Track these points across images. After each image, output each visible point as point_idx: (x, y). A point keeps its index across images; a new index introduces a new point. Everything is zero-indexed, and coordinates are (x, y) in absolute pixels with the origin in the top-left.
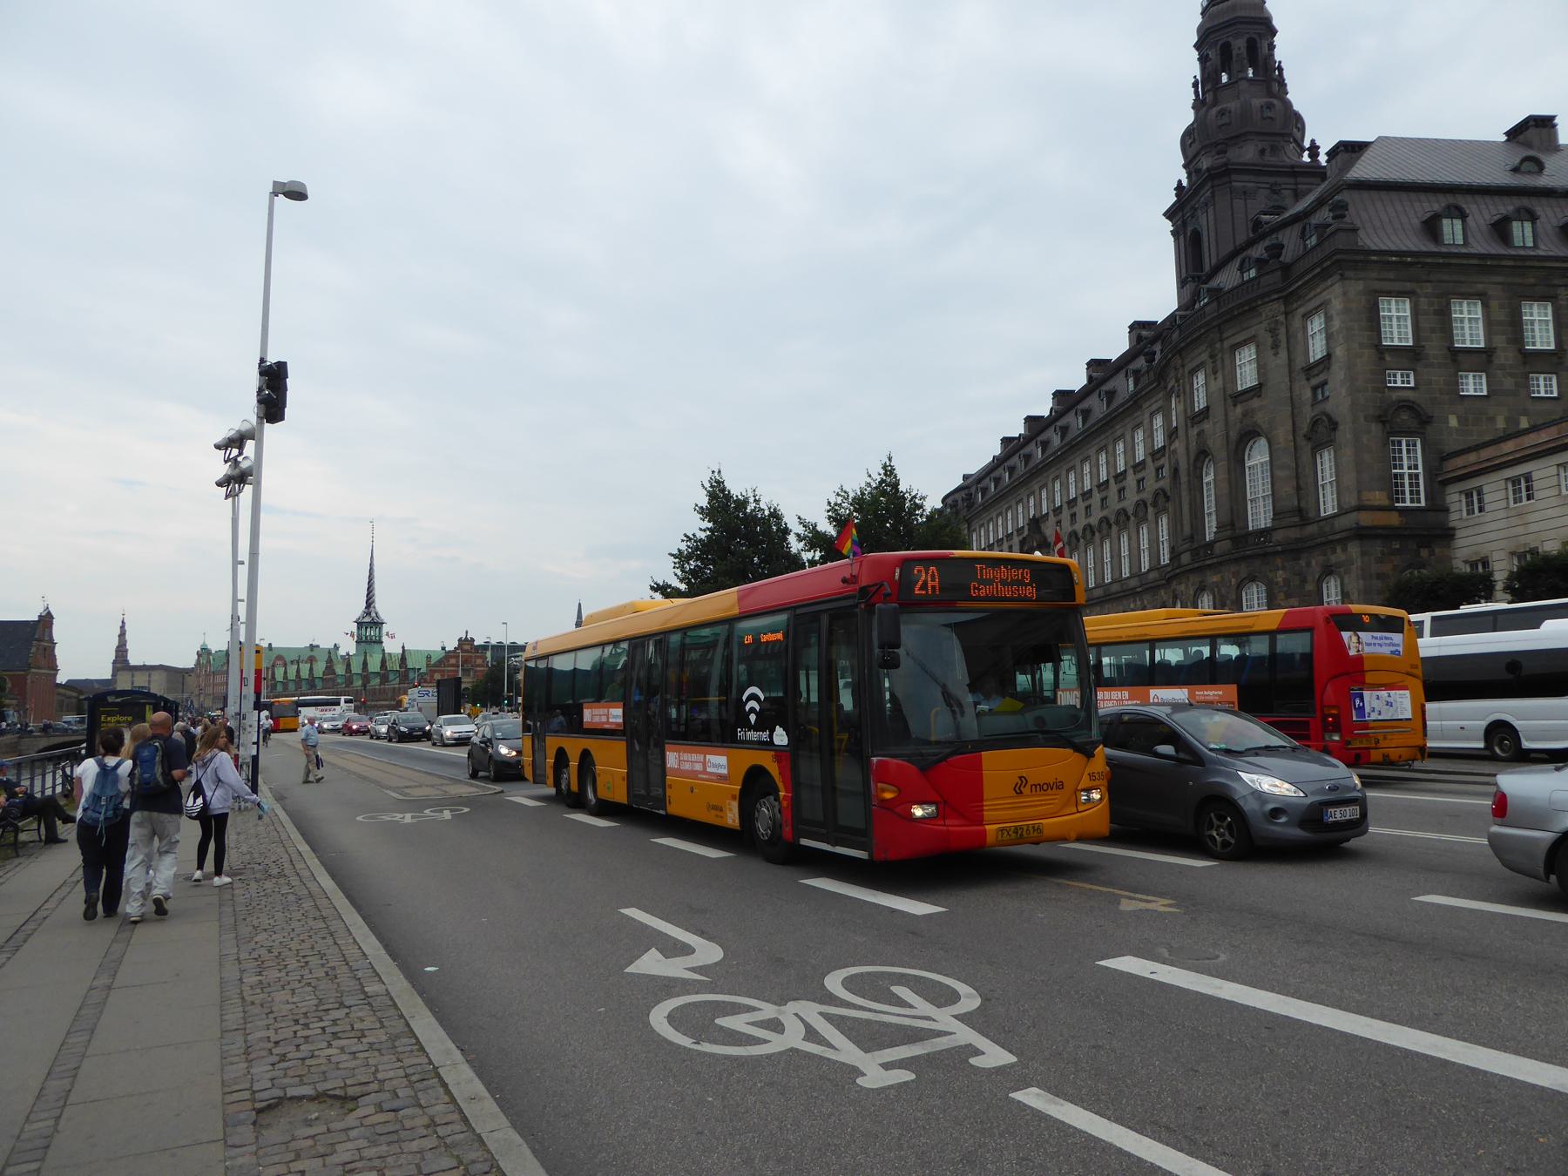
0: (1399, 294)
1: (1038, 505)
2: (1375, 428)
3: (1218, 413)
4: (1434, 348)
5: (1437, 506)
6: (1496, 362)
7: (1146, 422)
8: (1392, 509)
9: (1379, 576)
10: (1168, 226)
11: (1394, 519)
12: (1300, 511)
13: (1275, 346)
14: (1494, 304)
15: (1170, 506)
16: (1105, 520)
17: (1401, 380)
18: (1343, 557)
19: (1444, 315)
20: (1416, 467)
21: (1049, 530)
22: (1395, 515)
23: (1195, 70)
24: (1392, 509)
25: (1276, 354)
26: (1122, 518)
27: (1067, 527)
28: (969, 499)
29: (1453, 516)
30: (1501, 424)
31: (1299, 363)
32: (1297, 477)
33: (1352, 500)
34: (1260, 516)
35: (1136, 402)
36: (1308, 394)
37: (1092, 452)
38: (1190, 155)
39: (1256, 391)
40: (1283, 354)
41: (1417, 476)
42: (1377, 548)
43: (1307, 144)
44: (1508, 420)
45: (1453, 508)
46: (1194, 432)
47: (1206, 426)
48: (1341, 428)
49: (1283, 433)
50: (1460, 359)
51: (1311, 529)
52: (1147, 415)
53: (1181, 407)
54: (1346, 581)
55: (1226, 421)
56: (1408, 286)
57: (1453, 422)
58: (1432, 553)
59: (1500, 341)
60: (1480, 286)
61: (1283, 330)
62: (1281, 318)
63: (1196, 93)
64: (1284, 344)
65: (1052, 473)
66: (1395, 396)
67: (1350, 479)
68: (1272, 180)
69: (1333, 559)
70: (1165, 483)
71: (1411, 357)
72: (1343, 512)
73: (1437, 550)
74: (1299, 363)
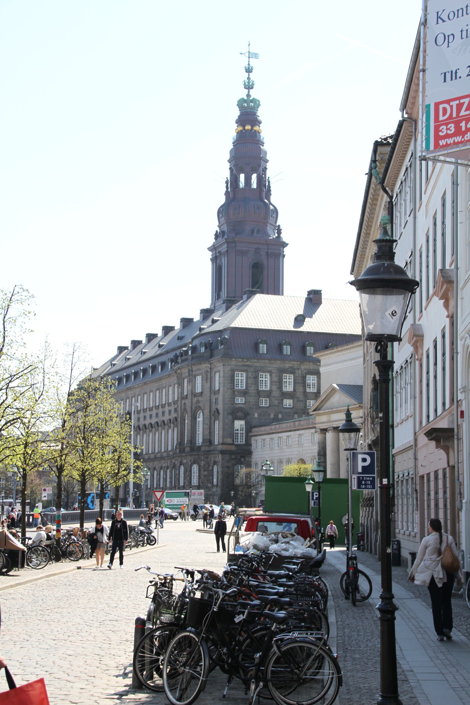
0: (242, 371)
2: (230, 417)
4: (252, 390)
5: (248, 443)
6: (272, 395)
7: (173, 386)
8: (233, 444)
9: (227, 467)
10: (209, 255)
11: (233, 448)
14: (274, 375)
16: (157, 423)
17: (240, 400)
19: (256, 378)
20: (243, 430)
22: (234, 446)
23: (227, 174)
24: (233, 444)
25: (207, 383)
29: (253, 448)
30: (272, 416)
32: (210, 429)
33: (221, 442)
34: (199, 440)
36: (214, 401)
38: (221, 224)
40: (209, 384)
41: (243, 434)
42: (227, 457)
43: (278, 224)
44: (275, 415)
45: (253, 445)
49: (207, 411)
50: (259, 394)
51: (212, 448)
52: (173, 384)
56: (245, 368)
57: (256, 415)
58: (245, 460)
59: (274, 388)
60: (270, 369)
61: (209, 374)
62: (209, 370)
63: (227, 187)
66: (237, 406)
71: (244, 393)
72: (219, 444)
73: (247, 459)
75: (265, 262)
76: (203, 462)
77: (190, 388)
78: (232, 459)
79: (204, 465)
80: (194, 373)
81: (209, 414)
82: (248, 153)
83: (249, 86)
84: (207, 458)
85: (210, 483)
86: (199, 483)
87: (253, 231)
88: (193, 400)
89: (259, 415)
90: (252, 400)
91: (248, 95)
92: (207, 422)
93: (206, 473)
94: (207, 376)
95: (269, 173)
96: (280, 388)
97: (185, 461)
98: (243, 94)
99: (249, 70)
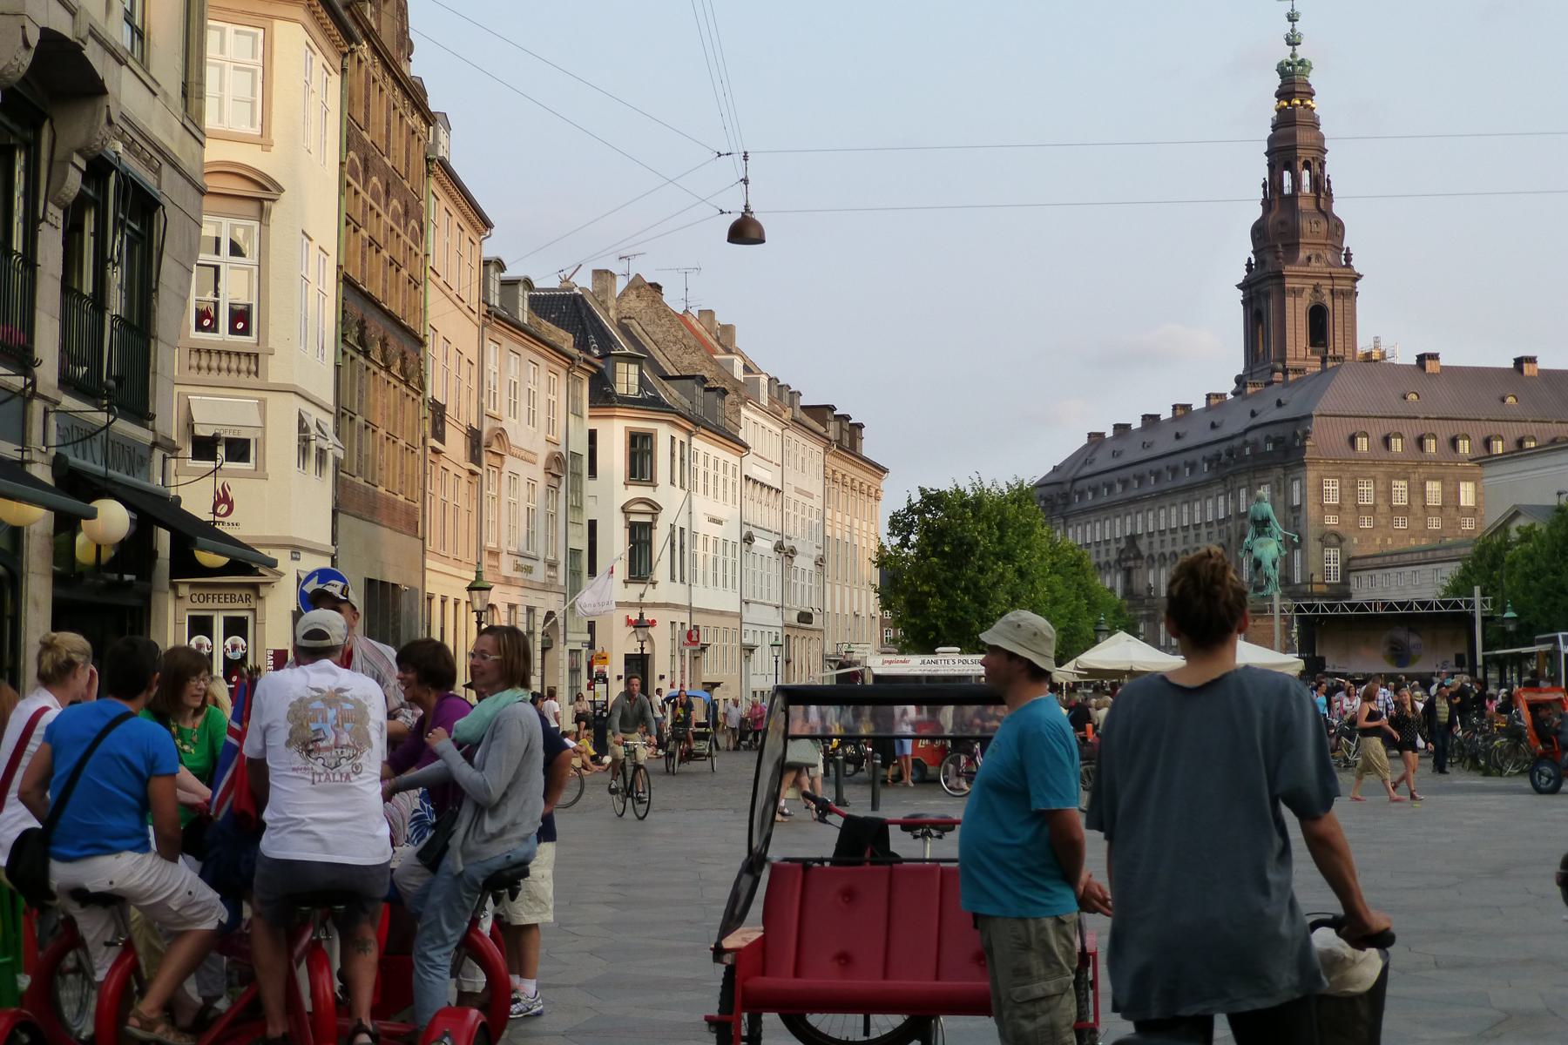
1: (1134, 525)
4: (1348, 504)
5: (1345, 582)
11: (1325, 589)
17: (1331, 521)
19: (1355, 487)
21: (1143, 546)
23: (1264, 172)
27: (1157, 549)
28: (1066, 497)
35: (1207, 484)
37: (1179, 501)
59: (1380, 501)
65: (1147, 505)
68: (1315, 282)
70: (1224, 540)
71: (1339, 509)
75: (1329, 304)
82: (1293, 142)
87: (1309, 259)
89: (1360, 540)
90: (1349, 519)
91: (1292, 56)
95: (1328, 170)
96: (1390, 500)
98: (1285, 53)
99: (1292, 18)
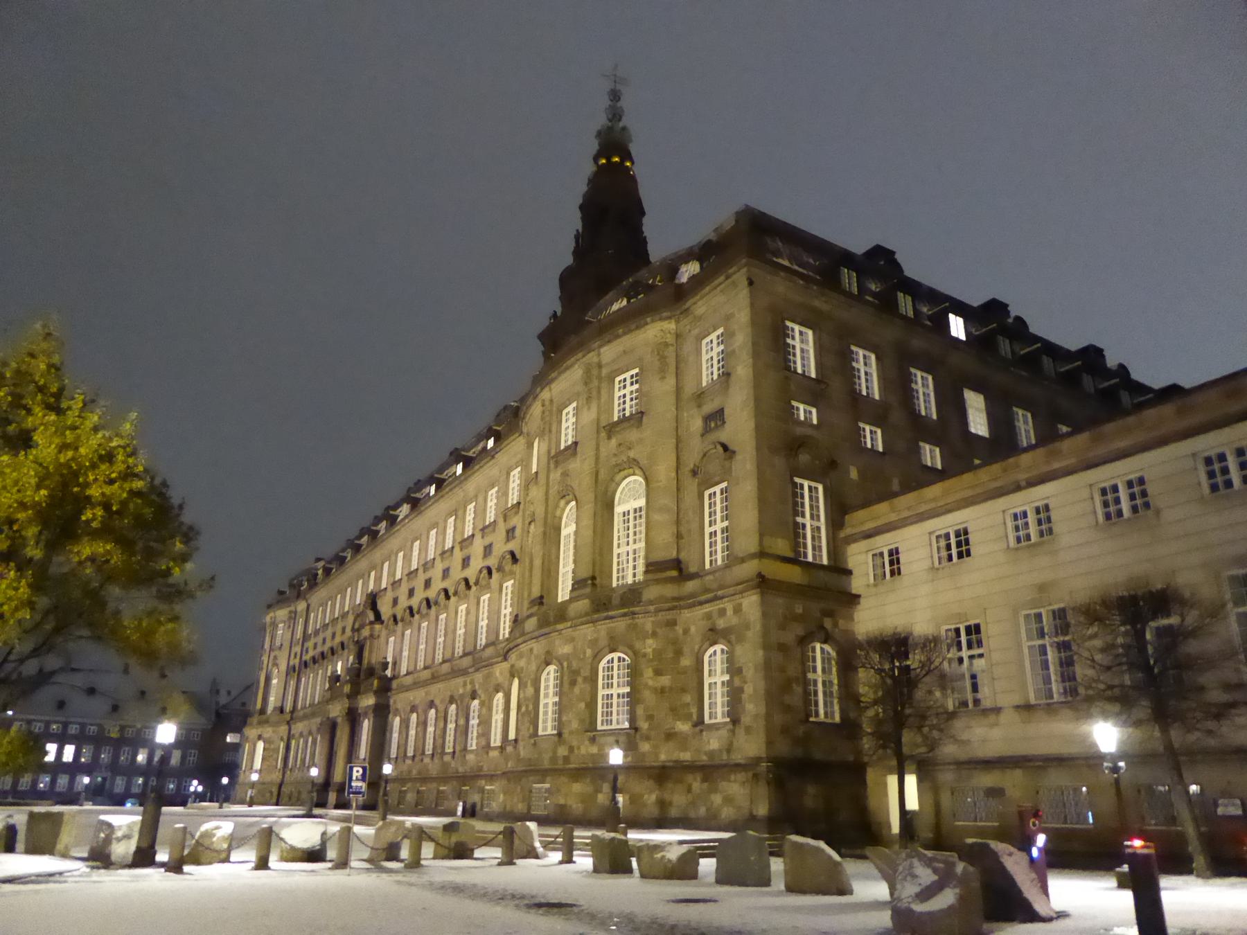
1: (378, 579)
2: (779, 462)
3: (587, 451)
5: (840, 569)
12: (677, 564)
13: (662, 371)
15: (517, 568)
18: (734, 621)
21: (385, 608)
26: (463, 585)
31: (689, 389)
32: (678, 522)
39: (638, 418)
40: (671, 381)
46: (556, 475)
47: (574, 465)
48: (739, 457)
49: (664, 470)
50: (857, 405)
51: (691, 586)
53: (545, 447)
54: (739, 650)
55: (597, 458)
58: (835, 625)
64: (672, 369)
67: (749, 518)
69: (721, 623)
74: (689, 389)
76: (650, 641)
77: (590, 416)
78: (797, 618)
79: (658, 653)
80: (604, 371)
81: (674, 474)
83: (615, 114)
84: (672, 624)
85: (688, 717)
86: (632, 720)
88: (602, 449)
89: (861, 473)
92: (668, 501)
93: (665, 680)
94: (662, 358)
97: (566, 649)
